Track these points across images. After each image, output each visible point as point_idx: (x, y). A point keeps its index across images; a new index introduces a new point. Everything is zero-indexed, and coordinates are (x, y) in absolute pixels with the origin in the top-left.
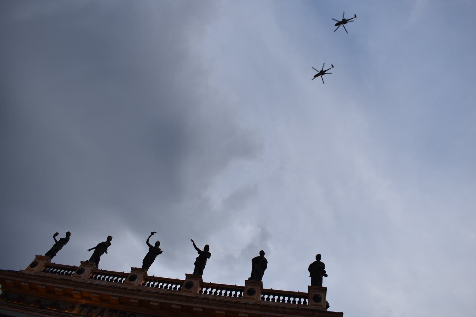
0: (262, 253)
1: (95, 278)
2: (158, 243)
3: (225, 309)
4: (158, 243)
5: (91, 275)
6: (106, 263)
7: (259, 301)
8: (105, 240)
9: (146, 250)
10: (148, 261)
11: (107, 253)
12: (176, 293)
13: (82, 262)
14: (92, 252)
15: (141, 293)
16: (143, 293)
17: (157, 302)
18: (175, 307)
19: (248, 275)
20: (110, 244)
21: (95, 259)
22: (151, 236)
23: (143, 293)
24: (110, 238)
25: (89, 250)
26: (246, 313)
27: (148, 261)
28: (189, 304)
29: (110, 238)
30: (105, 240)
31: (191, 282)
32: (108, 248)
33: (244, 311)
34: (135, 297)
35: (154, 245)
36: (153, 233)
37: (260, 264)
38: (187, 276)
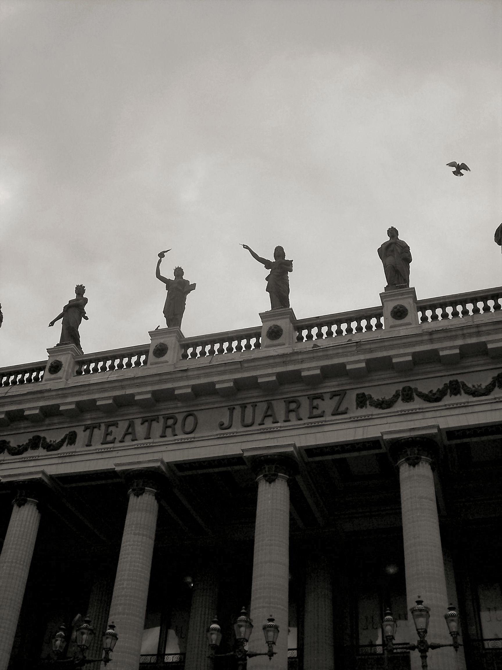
0: (393, 232)
1: (87, 371)
2: (179, 272)
3: (362, 357)
4: (179, 272)
5: (77, 368)
6: (93, 338)
7: (420, 326)
8: (74, 296)
9: (161, 295)
10: (174, 310)
11: (86, 318)
12: (253, 356)
13: (49, 351)
14: (59, 324)
15: (190, 373)
19: (381, 282)
20: (86, 301)
21: (71, 335)
24: (80, 290)
25: (52, 324)
27: (174, 310)
28: (291, 368)
29: (80, 290)
30: (74, 296)
31: (276, 326)
32: (86, 308)
34: (182, 384)
35: (173, 278)
37: (396, 256)
38: (264, 316)
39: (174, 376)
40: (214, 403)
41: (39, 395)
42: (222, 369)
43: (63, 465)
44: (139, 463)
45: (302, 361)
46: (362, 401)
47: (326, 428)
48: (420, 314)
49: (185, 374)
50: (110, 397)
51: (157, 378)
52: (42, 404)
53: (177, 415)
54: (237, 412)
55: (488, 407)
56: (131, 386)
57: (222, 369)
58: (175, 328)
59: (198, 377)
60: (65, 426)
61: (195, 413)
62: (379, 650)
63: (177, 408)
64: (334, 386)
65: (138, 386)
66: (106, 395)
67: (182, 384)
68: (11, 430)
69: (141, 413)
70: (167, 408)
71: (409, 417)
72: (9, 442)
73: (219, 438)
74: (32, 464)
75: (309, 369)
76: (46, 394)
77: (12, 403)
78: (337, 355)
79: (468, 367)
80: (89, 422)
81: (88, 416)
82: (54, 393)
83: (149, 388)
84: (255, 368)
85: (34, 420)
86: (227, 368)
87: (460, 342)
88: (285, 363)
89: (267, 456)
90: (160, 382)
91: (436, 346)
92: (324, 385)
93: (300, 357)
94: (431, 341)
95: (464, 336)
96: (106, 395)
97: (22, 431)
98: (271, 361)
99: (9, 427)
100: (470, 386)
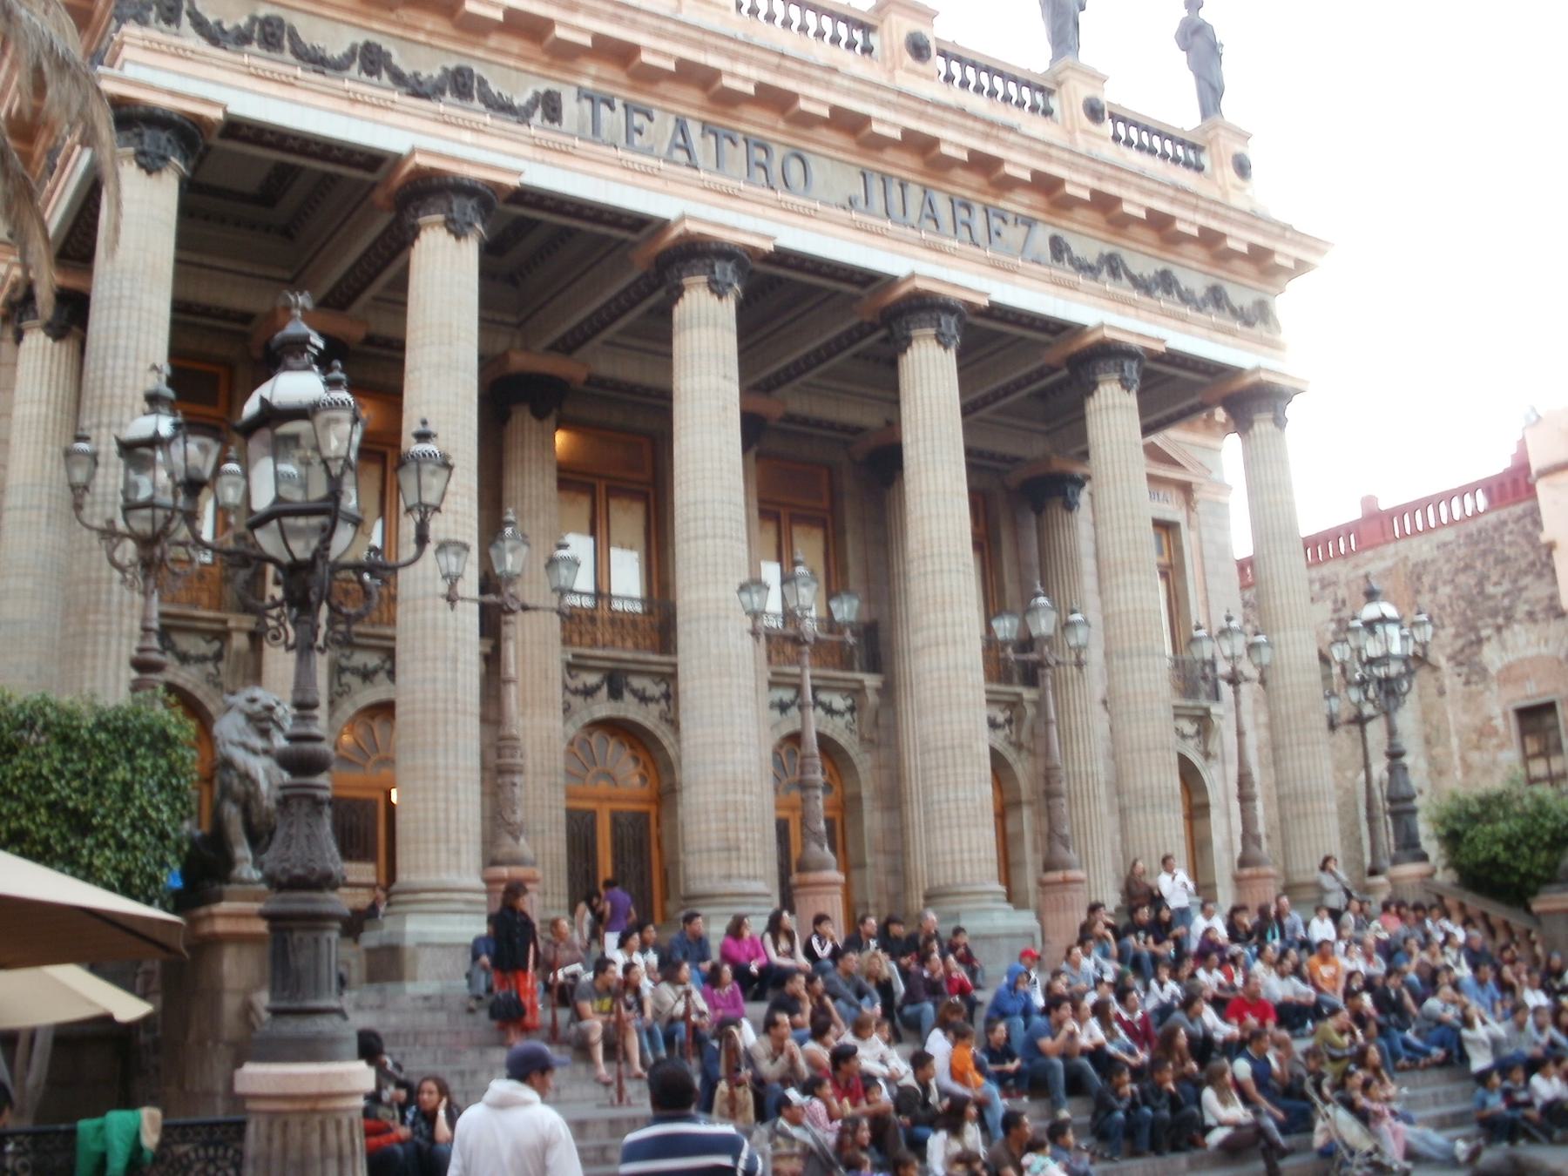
15: (837, 79)
16: (846, 83)
17: (894, 125)
26: (1140, 206)
33: (1137, 197)
40: (838, 148)
44: (735, 229)
47: (1018, 279)
49: (827, 76)
51: (775, 60)
56: (718, 50)
59: (849, 93)
61: (806, 156)
63: (773, 129)
64: (1022, 205)
66: (665, 46)
69: (701, 108)
70: (756, 122)
71: (1121, 307)
74: (467, 136)
75: (1016, 164)
80: (587, 83)
84: (942, 123)
87: (1201, 220)
88: (986, 137)
90: (778, 69)
93: (1012, 137)
94: (1173, 200)
96: (665, 46)
97: (421, 37)
99: (393, 16)
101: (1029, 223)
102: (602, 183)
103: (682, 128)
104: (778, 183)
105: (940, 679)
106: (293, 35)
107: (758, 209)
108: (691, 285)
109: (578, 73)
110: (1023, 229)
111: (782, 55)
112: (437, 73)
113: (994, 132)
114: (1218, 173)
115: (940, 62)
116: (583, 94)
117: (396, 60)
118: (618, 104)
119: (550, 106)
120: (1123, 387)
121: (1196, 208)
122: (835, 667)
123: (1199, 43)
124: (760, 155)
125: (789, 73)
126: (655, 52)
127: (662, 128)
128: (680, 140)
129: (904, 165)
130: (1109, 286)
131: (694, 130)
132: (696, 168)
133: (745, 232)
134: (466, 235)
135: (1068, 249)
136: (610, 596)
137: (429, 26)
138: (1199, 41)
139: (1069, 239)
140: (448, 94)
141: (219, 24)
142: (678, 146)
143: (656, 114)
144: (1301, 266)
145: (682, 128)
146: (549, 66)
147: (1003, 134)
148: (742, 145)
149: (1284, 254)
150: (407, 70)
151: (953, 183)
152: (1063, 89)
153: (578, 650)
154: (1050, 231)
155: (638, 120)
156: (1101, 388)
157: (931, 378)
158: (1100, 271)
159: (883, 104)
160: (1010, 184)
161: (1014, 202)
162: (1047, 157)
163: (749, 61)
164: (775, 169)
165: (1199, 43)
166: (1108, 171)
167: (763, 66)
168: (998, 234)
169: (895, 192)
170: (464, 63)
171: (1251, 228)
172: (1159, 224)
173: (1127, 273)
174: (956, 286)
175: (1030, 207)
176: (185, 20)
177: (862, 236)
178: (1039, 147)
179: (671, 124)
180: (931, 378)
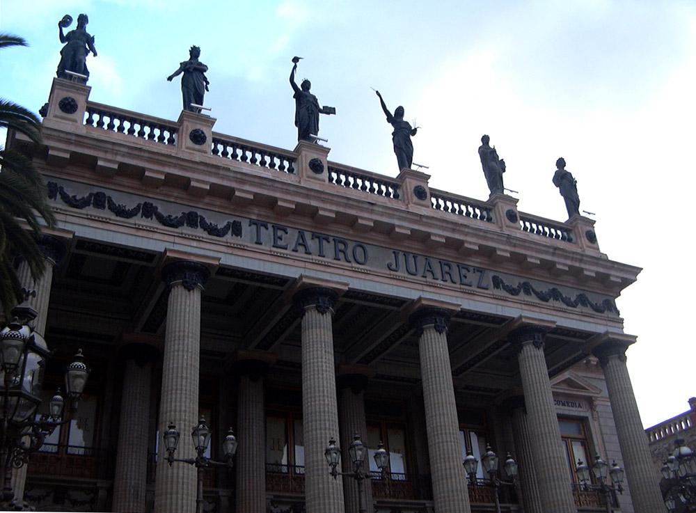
2: (306, 85)
3: (508, 248)
4: (306, 85)
8: (187, 58)
11: (208, 90)
15: (376, 208)
16: (381, 210)
18: (438, 239)
22: (295, 67)
23: (381, 210)
24: (195, 52)
25: (170, 79)
26: (536, 258)
28: (457, 236)
29: (195, 52)
34: (366, 215)
36: (296, 60)
39: (360, 205)
41: (214, 170)
42: (404, 215)
43: (233, 256)
45: (467, 234)
46: (497, 283)
48: (87, 115)
49: (371, 207)
50: (293, 201)
51: (344, 201)
52: (214, 180)
53: (349, 242)
54: (401, 257)
55: (578, 317)
56: (316, 198)
57: (404, 215)
58: (499, 193)
59: (382, 214)
60: (227, 212)
61: (365, 245)
62: (285, 470)
64: (477, 262)
65: (323, 201)
66: (289, 197)
67: (366, 215)
68: (157, 194)
72: (157, 208)
73: (313, 263)
74: (195, 244)
75: (470, 243)
76: (221, 172)
77: (175, 166)
78: (492, 240)
79: (563, 281)
81: (256, 211)
82: (232, 174)
83: (334, 208)
84: (431, 226)
85: (106, 174)
86: (409, 216)
87: (569, 262)
88: (454, 230)
89: (190, 262)
90: (346, 205)
91: (556, 259)
92: (473, 259)
93: (466, 230)
94: (553, 254)
95: (572, 259)
96: (289, 197)
97: (172, 200)
98: (445, 225)
99: (158, 190)
100: (564, 296)
101: (481, 270)
102: (262, 262)
103: (302, 236)
104: (351, 258)
105: (444, 497)
106: (110, 200)
107: (341, 272)
108: (308, 309)
109: (249, 213)
110: (479, 274)
111: (348, 199)
112: (180, 215)
113: (458, 228)
114: (579, 240)
115: (434, 200)
116: (252, 222)
117: (160, 210)
118: (270, 226)
119: (237, 230)
120: (536, 347)
121: (566, 258)
122: (411, 498)
123: (565, 182)
124: (341, 246)
125: (351, 207)
126: (285, 201)
127: (291, 237)
128: (301, 241)
129: (416, 247)
130: (527, 298)
131: (308, 236)
132: (310, 254)
133: (333, 282)
134: (193, 289)
135: (502, 282)
136: (295, 466)
137: (176, 194)
138: (564, 181)
139: (501, 276)
140: (185, 225)
141: (74, 197)
142: (300, 244)
143: (288, 230)
144: (626, 283)
145: (302, 236)
146: (234, 210)
147: (463, 229)
148: (332, 243)
149: (615, 276)
150: (165, 215)
151: (440, 254)
152: (496, 208)
153: (277, 493)
154: (491, 274)
155: (280, 233)
156: (525, 348)
157: (435, 348)
158: (519, 291)
159: (401, 219)
160: (470, 253)
161: (472, 261)
162: (485, 238)
163: (332, 202)
164: (349, 252)
165: (565, 182)
166: (518, 242)
167: (338, 204)
168: (465, 277)
169: (411, 260)
170: (194, 210)
171: (597, 264)
172: (548, 267)
173: (534, 291)
174: (443, 302)
175: (480, 263)
176: (59, 196)
177: (394, 282)
178: (481, 234)
179: (296, 234)
180: (435, 348)
